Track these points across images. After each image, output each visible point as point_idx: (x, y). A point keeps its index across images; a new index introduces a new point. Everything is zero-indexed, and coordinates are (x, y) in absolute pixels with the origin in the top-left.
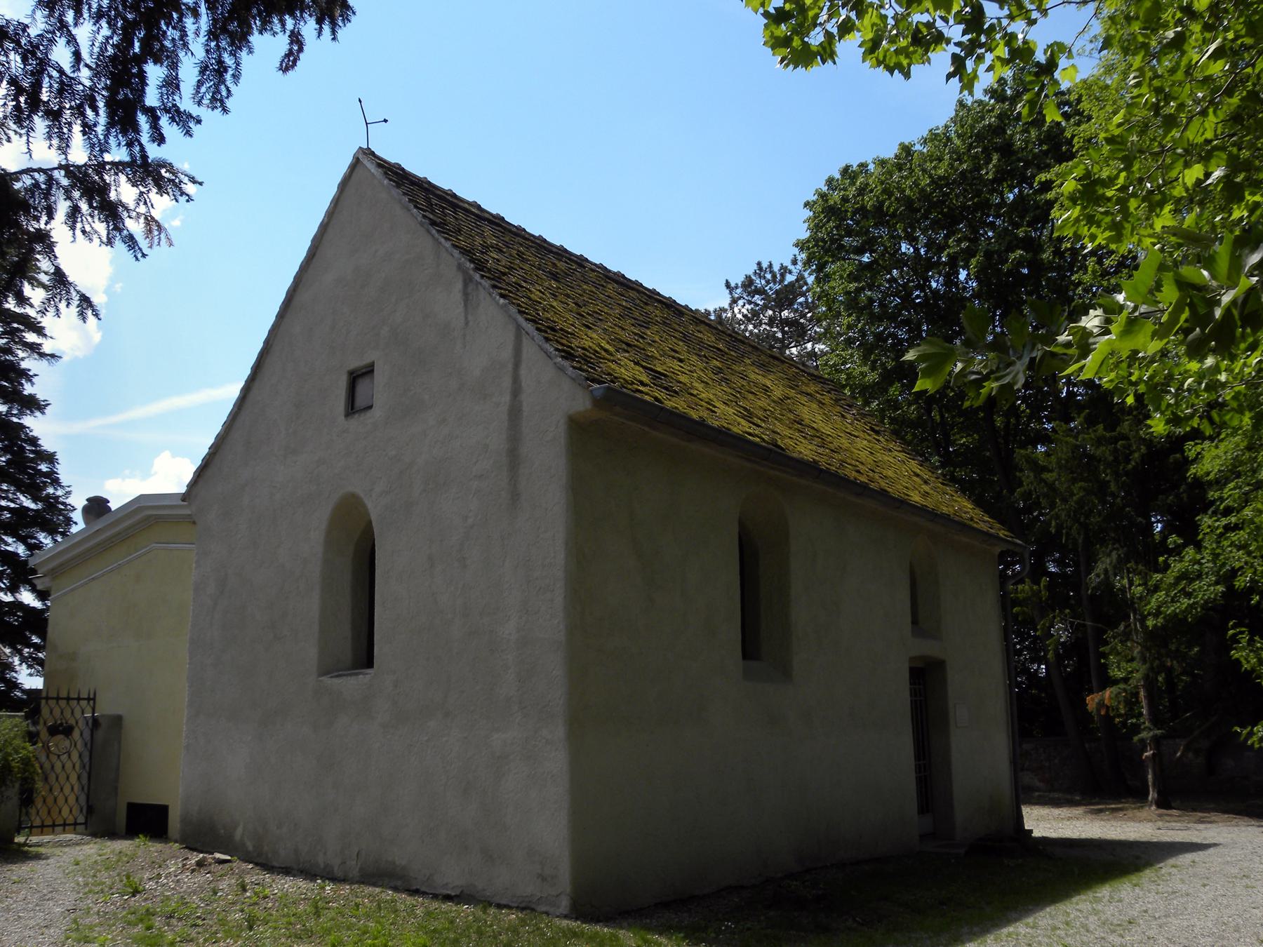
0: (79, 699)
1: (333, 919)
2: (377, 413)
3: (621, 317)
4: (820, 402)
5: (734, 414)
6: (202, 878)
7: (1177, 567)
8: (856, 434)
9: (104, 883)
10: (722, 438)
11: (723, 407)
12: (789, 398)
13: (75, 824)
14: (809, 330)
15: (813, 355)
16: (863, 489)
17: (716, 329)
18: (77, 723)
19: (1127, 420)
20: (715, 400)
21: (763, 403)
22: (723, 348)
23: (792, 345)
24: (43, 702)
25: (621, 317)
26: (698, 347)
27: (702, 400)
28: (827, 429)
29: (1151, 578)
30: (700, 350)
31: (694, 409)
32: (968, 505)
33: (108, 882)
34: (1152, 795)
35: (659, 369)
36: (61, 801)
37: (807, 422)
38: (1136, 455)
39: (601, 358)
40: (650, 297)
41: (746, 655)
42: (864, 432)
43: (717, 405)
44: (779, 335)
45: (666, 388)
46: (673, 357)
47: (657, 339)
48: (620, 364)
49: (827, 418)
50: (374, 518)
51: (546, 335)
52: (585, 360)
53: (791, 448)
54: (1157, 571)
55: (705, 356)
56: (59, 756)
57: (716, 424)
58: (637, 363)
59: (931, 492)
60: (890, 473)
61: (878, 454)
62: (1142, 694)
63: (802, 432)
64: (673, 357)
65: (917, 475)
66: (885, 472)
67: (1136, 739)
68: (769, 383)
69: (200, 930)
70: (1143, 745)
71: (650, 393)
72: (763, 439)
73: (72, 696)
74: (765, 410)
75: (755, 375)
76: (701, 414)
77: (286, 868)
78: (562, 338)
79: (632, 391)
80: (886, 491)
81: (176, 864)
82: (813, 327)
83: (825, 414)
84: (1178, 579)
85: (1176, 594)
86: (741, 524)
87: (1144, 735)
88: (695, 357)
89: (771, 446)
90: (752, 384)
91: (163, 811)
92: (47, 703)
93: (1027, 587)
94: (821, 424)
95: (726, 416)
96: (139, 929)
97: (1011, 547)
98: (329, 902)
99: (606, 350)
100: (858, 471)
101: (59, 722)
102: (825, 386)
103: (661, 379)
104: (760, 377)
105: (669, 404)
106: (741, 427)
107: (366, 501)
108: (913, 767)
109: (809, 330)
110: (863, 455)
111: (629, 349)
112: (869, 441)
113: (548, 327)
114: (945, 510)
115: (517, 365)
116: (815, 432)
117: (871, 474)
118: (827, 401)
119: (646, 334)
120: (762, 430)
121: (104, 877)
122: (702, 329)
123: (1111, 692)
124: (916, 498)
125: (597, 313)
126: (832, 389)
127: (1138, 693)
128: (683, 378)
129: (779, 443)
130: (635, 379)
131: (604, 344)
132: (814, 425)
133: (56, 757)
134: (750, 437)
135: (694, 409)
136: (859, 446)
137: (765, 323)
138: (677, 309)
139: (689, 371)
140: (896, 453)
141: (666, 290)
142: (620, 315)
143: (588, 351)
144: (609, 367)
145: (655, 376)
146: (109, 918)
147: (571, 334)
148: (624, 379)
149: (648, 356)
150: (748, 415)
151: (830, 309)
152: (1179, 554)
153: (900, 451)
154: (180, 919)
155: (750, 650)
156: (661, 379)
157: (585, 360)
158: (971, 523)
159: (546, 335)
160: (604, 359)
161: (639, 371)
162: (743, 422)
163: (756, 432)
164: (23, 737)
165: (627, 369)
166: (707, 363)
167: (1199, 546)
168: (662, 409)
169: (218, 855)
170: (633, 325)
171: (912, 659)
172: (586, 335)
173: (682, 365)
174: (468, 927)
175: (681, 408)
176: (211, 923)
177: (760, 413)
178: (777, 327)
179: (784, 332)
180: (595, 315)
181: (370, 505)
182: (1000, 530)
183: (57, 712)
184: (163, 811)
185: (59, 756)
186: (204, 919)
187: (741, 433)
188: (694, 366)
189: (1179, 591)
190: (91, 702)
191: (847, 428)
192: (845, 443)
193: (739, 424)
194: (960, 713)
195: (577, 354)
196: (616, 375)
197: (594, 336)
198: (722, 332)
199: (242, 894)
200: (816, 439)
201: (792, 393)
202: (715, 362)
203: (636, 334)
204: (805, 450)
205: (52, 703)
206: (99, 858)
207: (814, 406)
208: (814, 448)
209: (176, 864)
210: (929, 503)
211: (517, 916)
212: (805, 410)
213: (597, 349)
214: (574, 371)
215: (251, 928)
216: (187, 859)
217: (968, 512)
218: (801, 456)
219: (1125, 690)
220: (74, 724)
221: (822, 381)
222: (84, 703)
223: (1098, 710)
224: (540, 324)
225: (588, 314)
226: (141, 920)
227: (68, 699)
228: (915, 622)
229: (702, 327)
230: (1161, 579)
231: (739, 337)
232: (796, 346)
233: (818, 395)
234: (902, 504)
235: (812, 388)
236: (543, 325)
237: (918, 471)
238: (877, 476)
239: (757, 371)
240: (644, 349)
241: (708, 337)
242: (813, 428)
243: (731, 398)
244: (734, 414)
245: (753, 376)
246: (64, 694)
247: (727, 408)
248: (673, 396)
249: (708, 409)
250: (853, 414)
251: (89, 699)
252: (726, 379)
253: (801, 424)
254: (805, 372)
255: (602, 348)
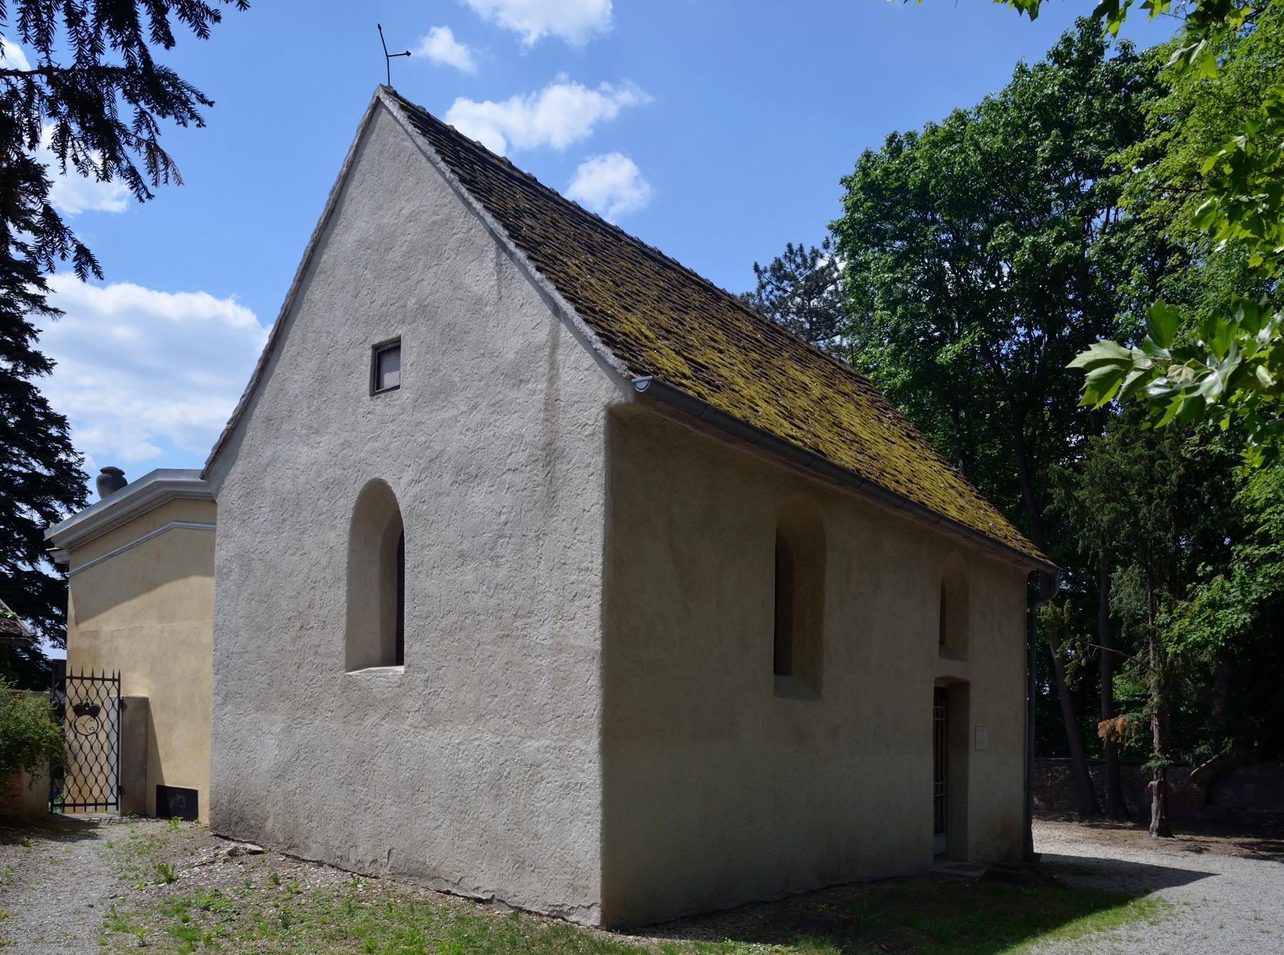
0: (103, 680)
1: (366, 920)
2: (405, 395)
3: (659, 300)
4: (857, 403)
5: (776, 414)
6: (235, 868)
7: (1204, 595)
8: (893, 440)
9: (138, 869)
10: (764, 439)
11: (764, 405)
12: (827, 398)
13: (107, 804)
14: (838, 321)
15: (839, 349)
16: (902, 502)
17: (754, 317)
18: (103, 704)
19: (1168, 438)
20: (756, 397)
21: (802, 402)
22: (761, 339)
23: (820, 337)
24: (68, 681)
25: (659, 300)
26: (736, 337)
27: (742, 396)
28: (865, 435)
29: (1177, 605)
30: (739, 340)
31: (736, 407)
32: (1002, 522)
33: (142, 868)
34: (1154, 823)
35: (700, 361)
36: (91, 780)
37: (845, 425)
38: (1174, 477)
39: (642, 345)
40: (687, 277)
41: (776, 672)
42: (901, 438)
43: (759, 402)
44: (807, 326)
45: (708, 383)
46: (714, 348)
47: (696, 326)
48: (661, 353)
49: (865, 423)
50: (401, 508)
51: (586, 317)
52: (627, 347)
53: (832, 454)
54: (1185, 599)
55: (744, 347)
56: (86, 736)
57: (759, 424)
58: (678, 353)
59: (967, 506)
60: (927, 484)
61: (915, 463)
62: (1155, 722)
63: (841, 436)
64: (714, 348)
65: (953, 487)
66: (922, 483)
67: (1143, 767)
68: (807, 381)
69: (235, 925)
70: (1149, 775)
71: (694, 388)
72: (805, 443)
73: (96, 676)
74: (805, 411)
75: (794, 371)
76: (744, 413)
77: (317, 862)
78: (602, 321)
79: (676, 384)
80: (924, 504)
81: (208, 852)
82: (843, 318)
83: (862, 416)
84: (1203, 607)
85: (1199, 622)
86: (779, 535)
87: (1152, 763)
88: (735, 348)
89: (812, 451)
90: (790, 380)
91: (192, 795)
92: (71, 682)
93: (1049, 609)
94: (859, 428)
95: (767, 416)
96: (174, 921)
97: (1042, 568)
98: (362, 901)
99: (646, 337)
100: (897, 482)
101: (84, 702)
102: (862, 386)
103: (702, 372)
104: (798, 373)
105: (714, 400)
106: (783, 429)
107: (394, 490)
108: (932, 788)
109: (838, 321)
110: (901, 463)
111: (669, 336)
112: (905, 448)
113: (587, 308)
114: (980, 526)
115: (554, 349)
116: (853, 436)
117: (909, 485)
118: (864, 402)
119: (685, 320)
120: (803, 433)
121: (136, 861)
122: (740, 317)
123: (1124, 720)
124: (953, 513)
125: (636, 294)
126: (869, 390)
127: (1149, 724)
128: (723, 371)
129: (821, 448)
130: (677, 370)
131: (644, 329)
132: (853, 429)
133: (84, 737)
134: (793, 441)
135: (736, 407)
136: (896, 454)
137: (793, 313)
138: (714, 293)
139: (731, 364)
140: (932, 462)
141: (705, 271)
142: (659, 298)
143: (628, 337)
144: (651, 356)
145: (698, 367)
146: (146, 907)
147: (611, 317)
148: (667, 371)
149: (688, 344)
150: (789, 416)
151: (860, 302)
152: (1208, 582)
153: (935, 460)
154: (215, 912)
155: (782, 665)
156: (702, 372)
157: (627, 347)
158: (1005, 541)
159: (586, 317)
160: (645, 346)
161: (680, 362)
162: (786, 424)
163: (798, 435)
164: (50, 716)
165: (671, 362)
166: (746, 355)
167: (1229, 575)
168: (707, 406)
169: (250, 846)
170: (672, 309)
171: (938, 680)
172: (626, 318)
173: (722, 356)
174: (503, 936)
175: (724, 406)
176: (245, 917)
177: (801, 414)
178: (806, 317)
179: (811, 323)
180: (634, 296)
181: (398, 495)
182: (1032, 549)
183: (82, 691)
184: (192, 795)
185: (86, 736)
186: (239, 914)
187: (784, 436)
188: (733, 358)
189: (1204, 620)
190: (116, 683)
191: (884, 433)
192: (882, 448)
193: (781, 425)
194: (979, 736)
195: (618, 340)
196: (659, 366)
197: (634, 319)
198: (760, 321)
199: (275, 888)
200: (856, 444)
201: (830, 392)
202: (754, 354)
203: (675, 320)
204: (846, 457)
205: (77, 682)
206: (131, 841)
207: (852, 407)
208: (853, 454)
209: (208, 852)
210: (964, 518)
211: (549, 925)
212: (844, 411)
213: (638, 335)
214: (616, 359)
215: (286, 926)
216: (218, 848)
217: (1002, 529)
218: (842, 462)
219: (1138, 719)
220: (100, 705)
221: (859, 379)
222: (108, 684)
223: (1109, 737)
224: (579, 304)
225: (626, 294)
226: (178, 911)
227: (93, 679)
228: (942, 642)
229: (740, 315)
230: (1187, 606)
231: (777, 328)
232: (823, 339)
233: (855, 396)
234: (939, 518)
235: (849, 387)
236: (582, 305)
237: (954, 484)
238: (915, 487)
239: (795, 366)
240: (684, 338)
241: (747, 327)
242: (852, 432)
243: (772, 395)
244: (776, 414)
245: (791, 372)
246: (87, 674)
247: (769, 407)
248: (715, 392)
249: (750, 407)
250: (889, 418)
251: (113, 680)
252: (766, 375)
253: (840, 427)
254: (842, 370)
255: (642, 333)
